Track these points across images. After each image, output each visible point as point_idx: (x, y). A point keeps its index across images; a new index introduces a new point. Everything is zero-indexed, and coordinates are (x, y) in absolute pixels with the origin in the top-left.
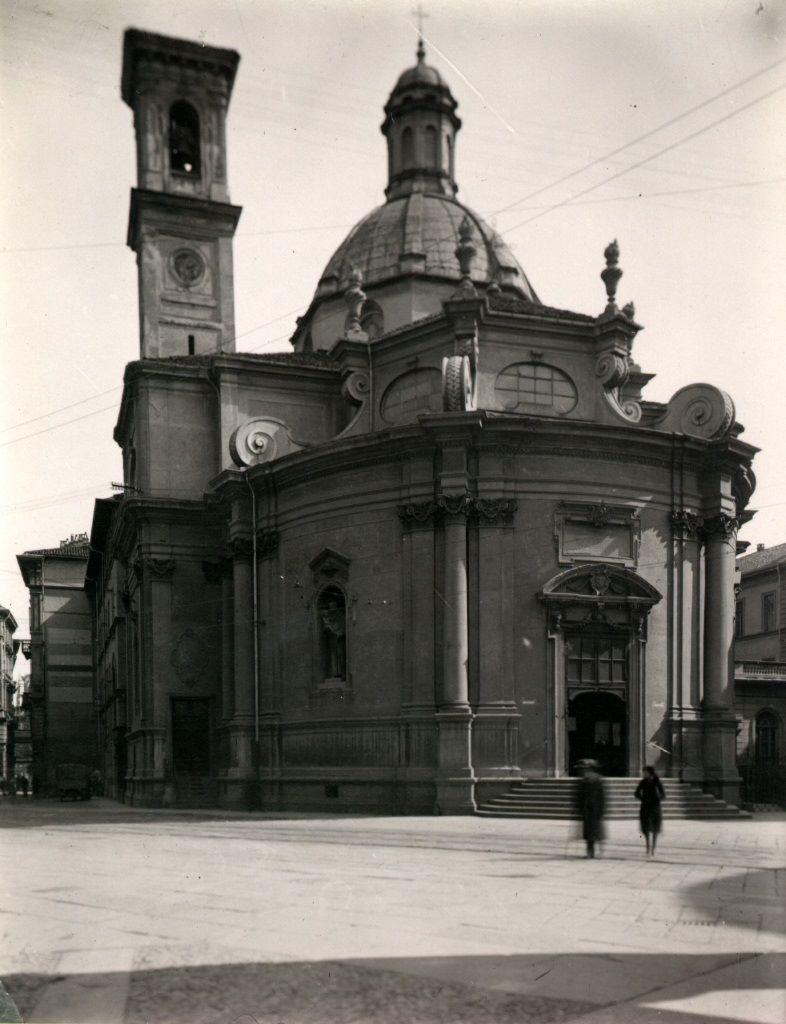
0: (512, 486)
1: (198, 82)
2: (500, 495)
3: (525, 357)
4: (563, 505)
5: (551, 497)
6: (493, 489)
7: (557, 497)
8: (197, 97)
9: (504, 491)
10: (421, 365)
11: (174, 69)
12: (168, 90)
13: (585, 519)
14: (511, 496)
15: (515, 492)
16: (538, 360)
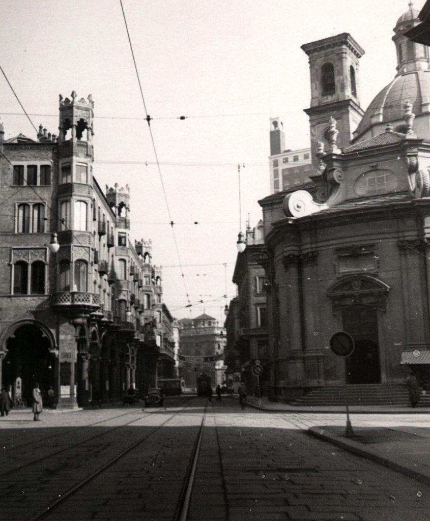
0: (314, 245)
1: (332, 52)
2: (310, 250)
3: (369, 169)
4: (338, 250)
5: (331, 247)
6: (307, 248)
7: (334, 247)
8: (332, 59)
9: (312, 248)
10: (379, 167)
11: (323, 52)
12: (320, 62)
13: (348, 254)
14: (314, 250)
15: (317, 247)
16: (374, 169)
